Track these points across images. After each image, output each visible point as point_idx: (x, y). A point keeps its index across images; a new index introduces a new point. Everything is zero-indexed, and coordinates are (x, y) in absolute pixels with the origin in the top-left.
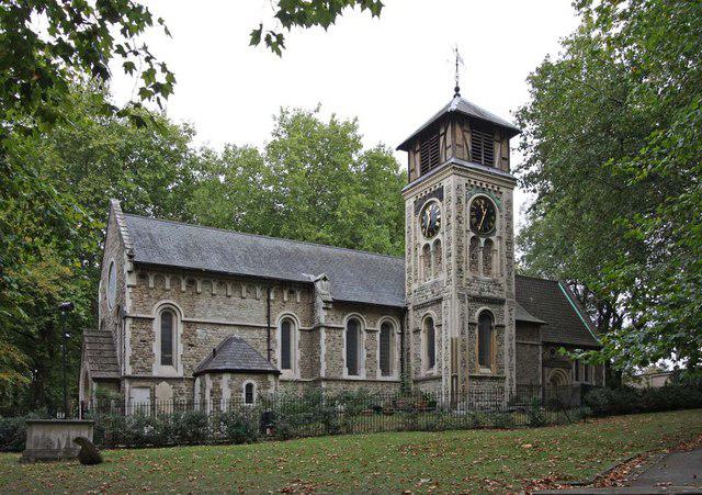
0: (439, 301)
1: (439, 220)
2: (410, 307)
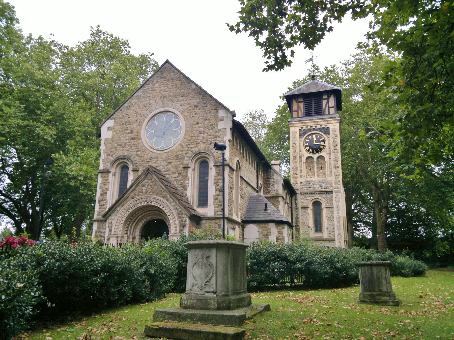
0: (331, 192)
1: (323, 146)
2: (298, 192)
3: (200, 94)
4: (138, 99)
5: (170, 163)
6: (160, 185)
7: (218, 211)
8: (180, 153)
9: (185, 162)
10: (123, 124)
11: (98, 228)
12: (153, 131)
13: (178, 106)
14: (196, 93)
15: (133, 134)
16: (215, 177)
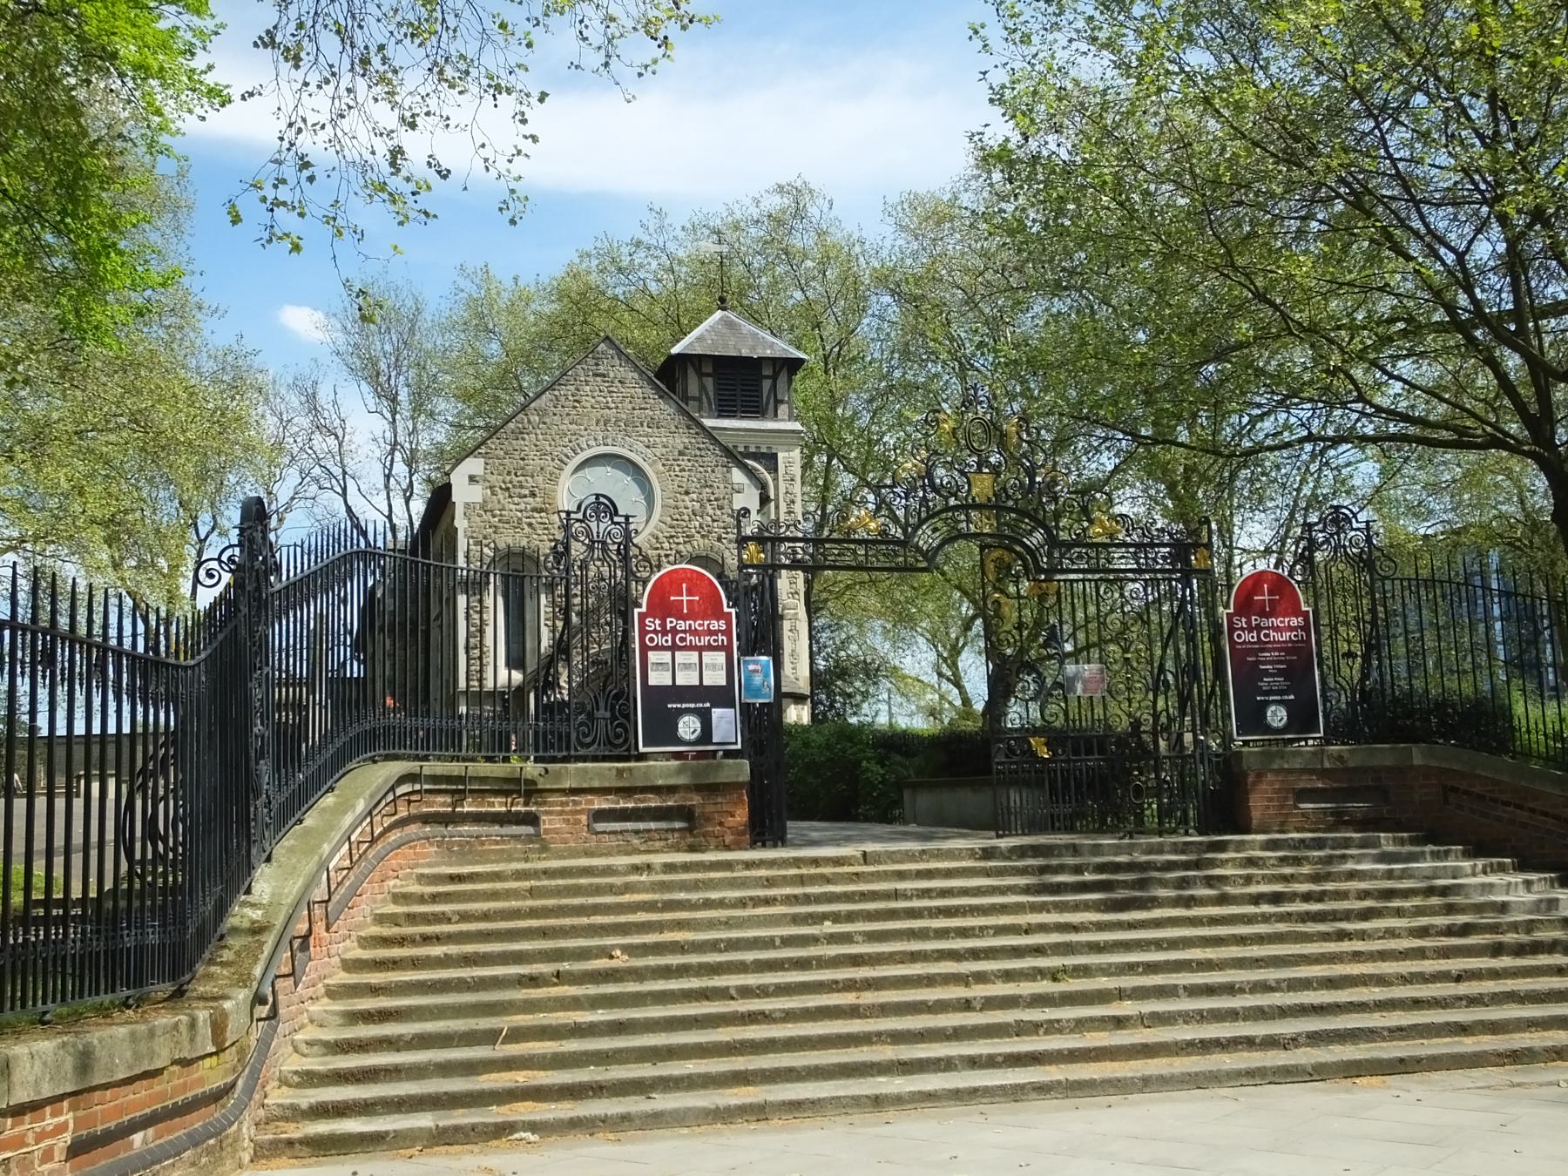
13: (641, 447)
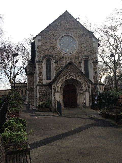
3: (84, 30)
4: (53, 28)
5: (73, 60)
6: (77, 70)
7: (95, 81)
8: (77, 56)
9: (80, 60)
10: (47, 39)
11: (40, 88)
12: (62, 45)
14: (81, 29)
15: (53, 45)
16: (93, 67)
